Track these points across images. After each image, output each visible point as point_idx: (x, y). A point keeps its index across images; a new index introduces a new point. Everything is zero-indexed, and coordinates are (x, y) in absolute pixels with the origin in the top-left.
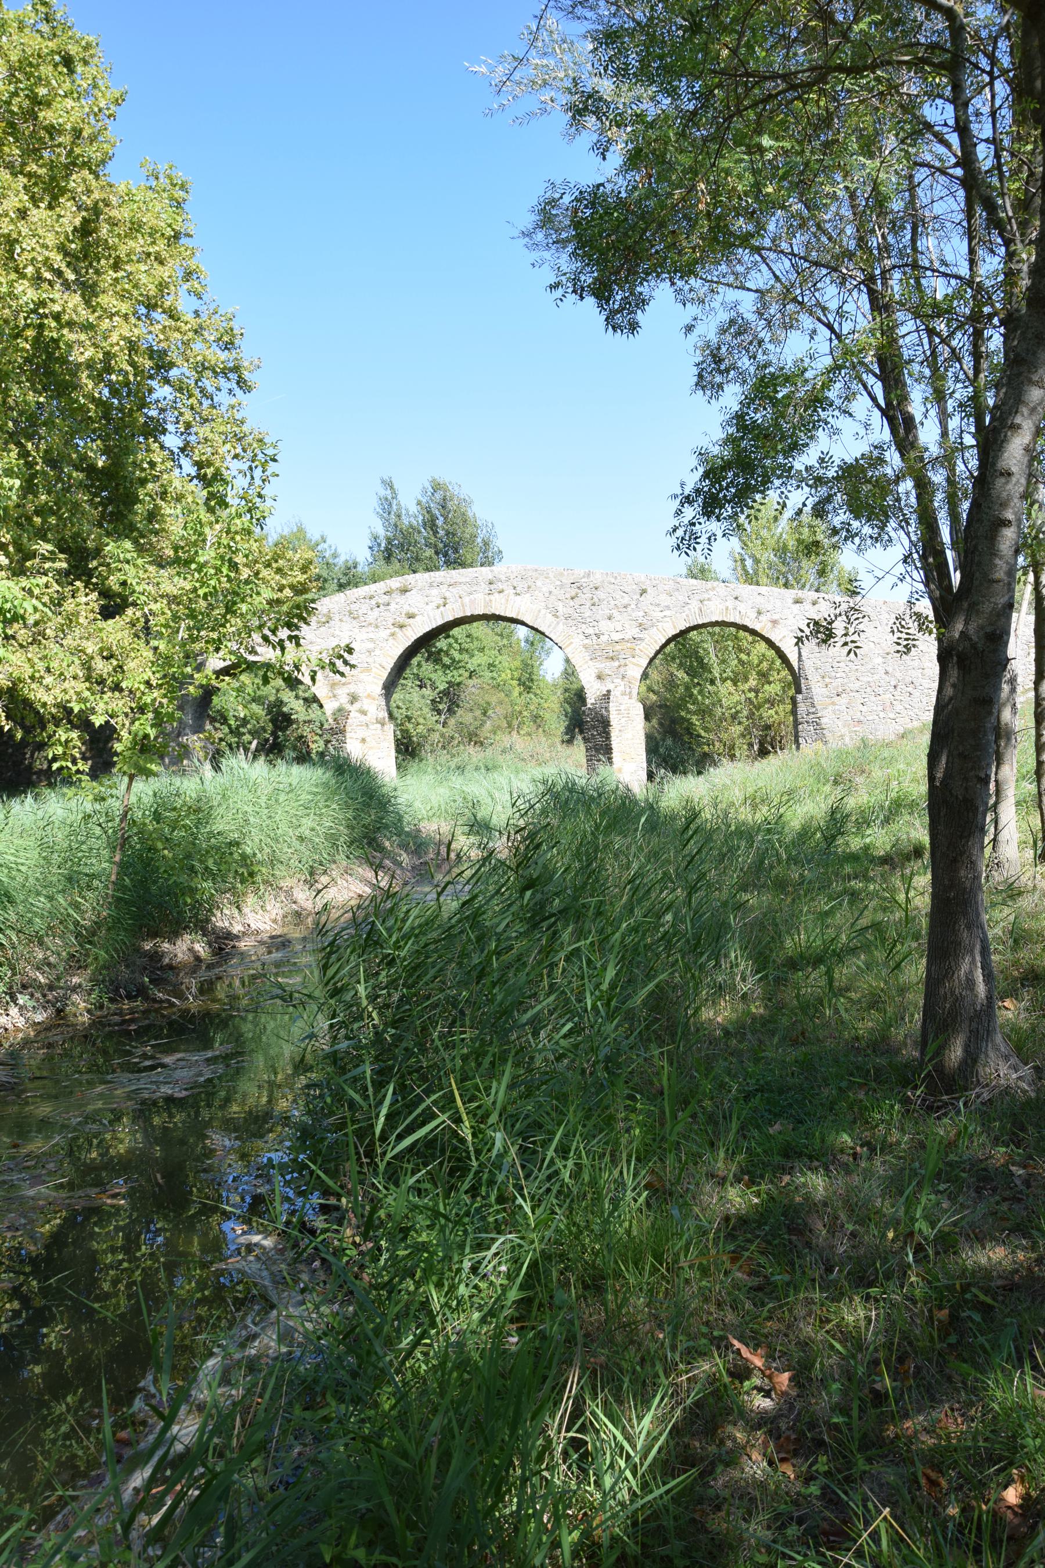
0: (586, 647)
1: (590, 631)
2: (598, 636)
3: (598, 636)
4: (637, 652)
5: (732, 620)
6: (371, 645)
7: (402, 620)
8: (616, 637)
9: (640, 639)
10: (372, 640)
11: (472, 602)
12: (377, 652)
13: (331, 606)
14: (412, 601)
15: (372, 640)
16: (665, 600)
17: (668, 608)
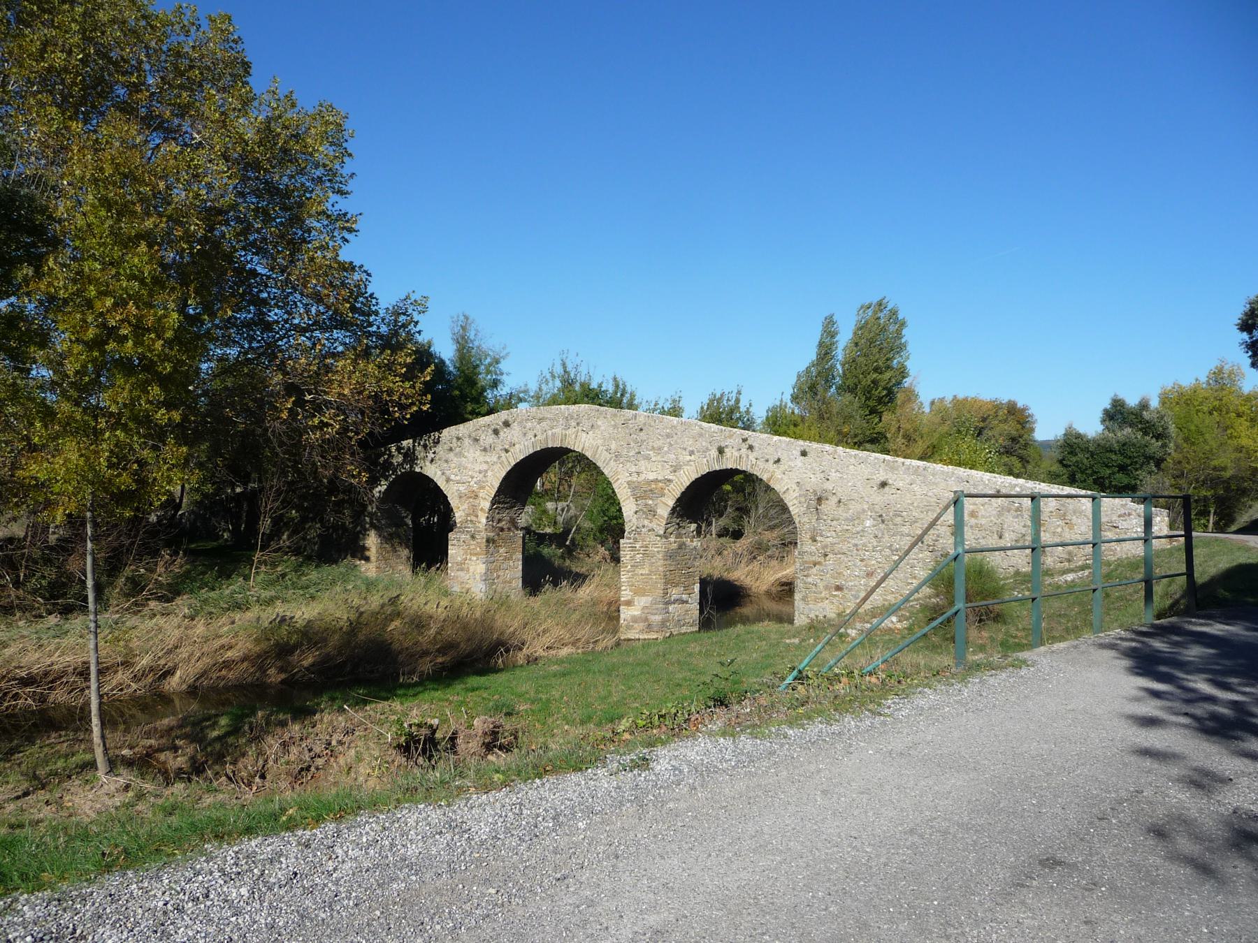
0: (629, 483)
1: (634, 469)
2: (638, 473)
3: (638, 473)
4: (666, 491)
5: (744, 469)
6: (485, 467)
7: (507, 447)
8: (652, 476)
9: (670, 481)
10: (487, 462)
11: (553, 435)
12: (489, 473)
13: (465, 431)
14: (513, 434)
15: (487, 462)
16: (689, 444)
17: (691, 453)
